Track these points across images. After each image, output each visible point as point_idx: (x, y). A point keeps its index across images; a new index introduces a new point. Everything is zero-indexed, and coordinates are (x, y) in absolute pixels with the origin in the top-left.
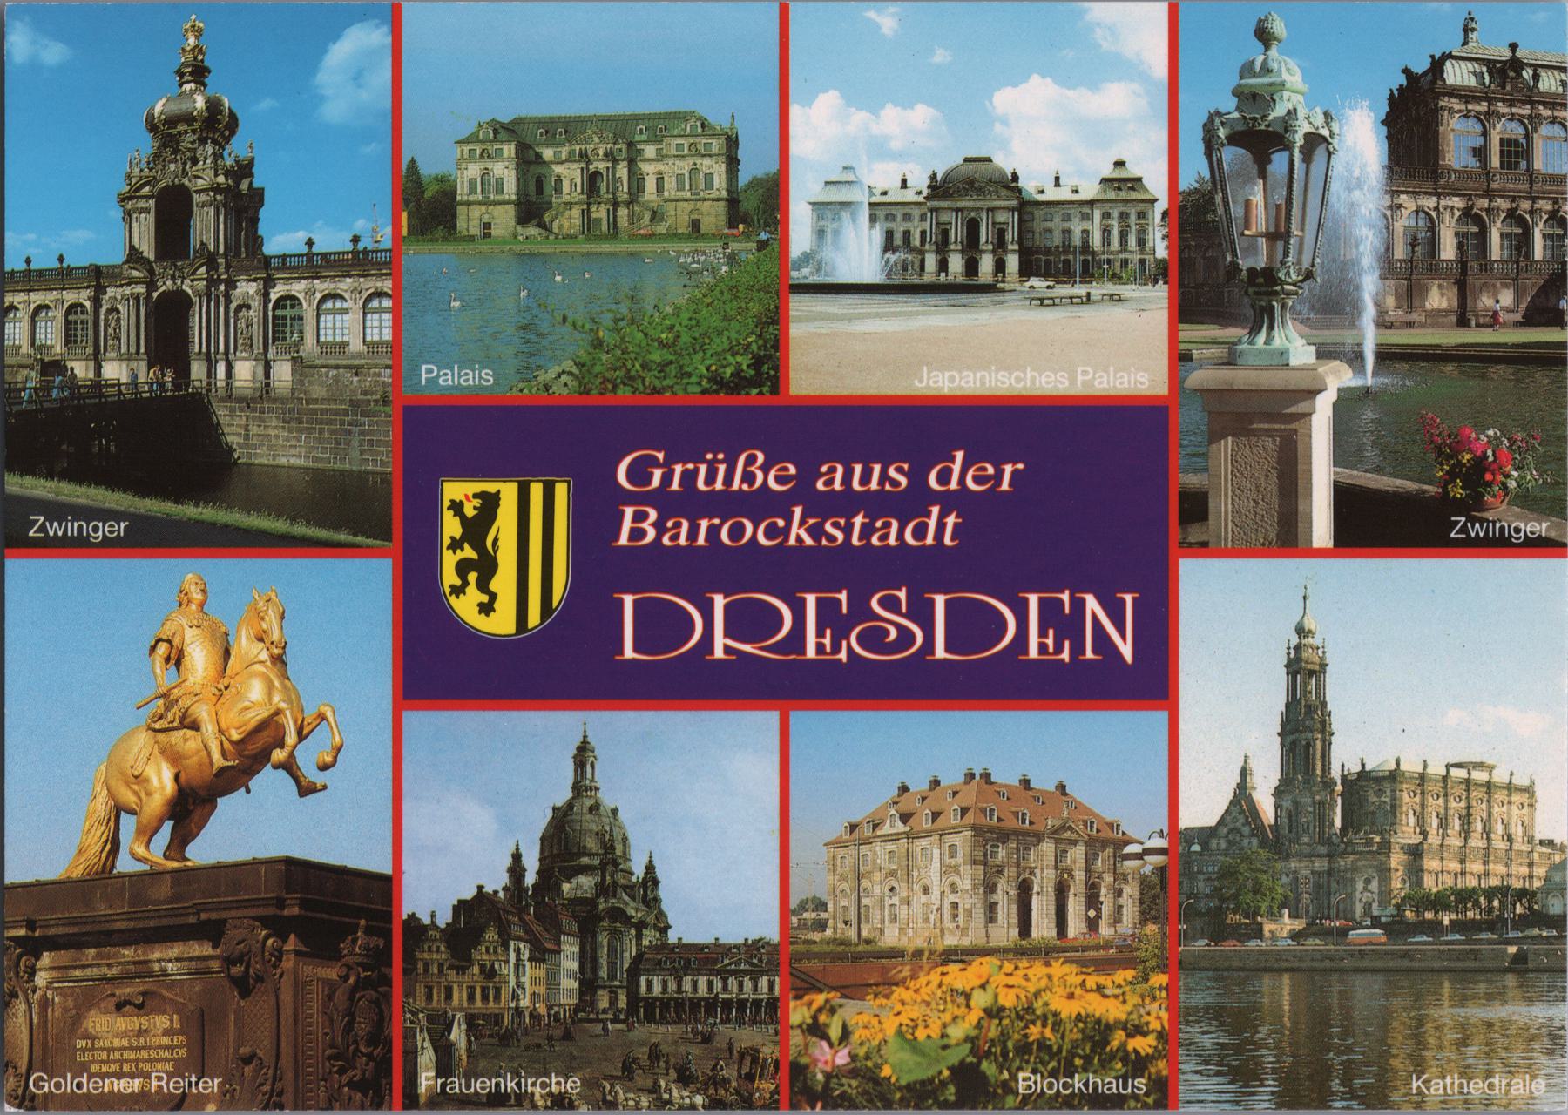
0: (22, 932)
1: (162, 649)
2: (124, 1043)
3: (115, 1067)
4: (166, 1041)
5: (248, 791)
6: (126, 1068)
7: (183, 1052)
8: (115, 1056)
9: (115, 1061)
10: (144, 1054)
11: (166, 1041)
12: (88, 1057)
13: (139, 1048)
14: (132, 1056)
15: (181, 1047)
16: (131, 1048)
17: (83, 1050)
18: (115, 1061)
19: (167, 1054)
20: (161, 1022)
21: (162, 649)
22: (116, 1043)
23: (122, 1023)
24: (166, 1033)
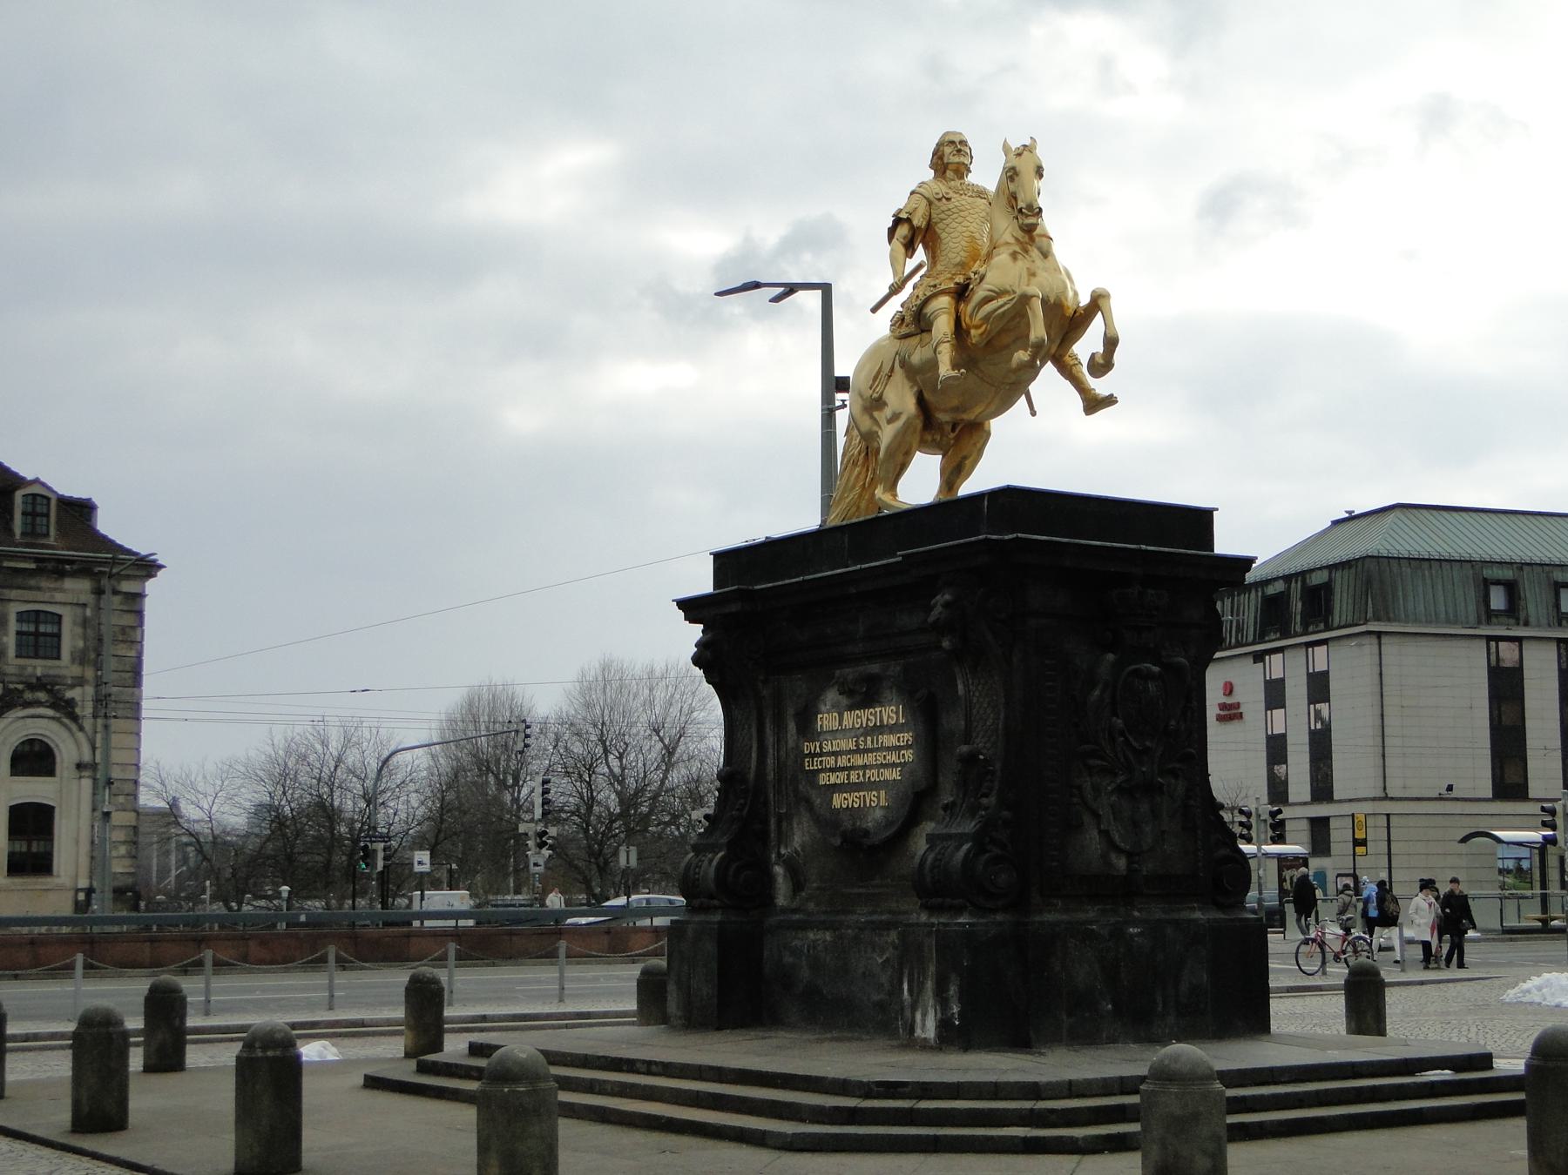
0: (734, 608)
1: (903, 230)
4: (889, 740)
5: (1033, 413)
6: (854, 778)
8: (842, 761)
10: (869, 759)
14: (860, 762)
15: (907, 747)
16: (858, 751)
17: (812, 755)
19: (893, 758)
20: (890, 713)
21: (903, 230)
23: (850, 719)
24: (893, 729)
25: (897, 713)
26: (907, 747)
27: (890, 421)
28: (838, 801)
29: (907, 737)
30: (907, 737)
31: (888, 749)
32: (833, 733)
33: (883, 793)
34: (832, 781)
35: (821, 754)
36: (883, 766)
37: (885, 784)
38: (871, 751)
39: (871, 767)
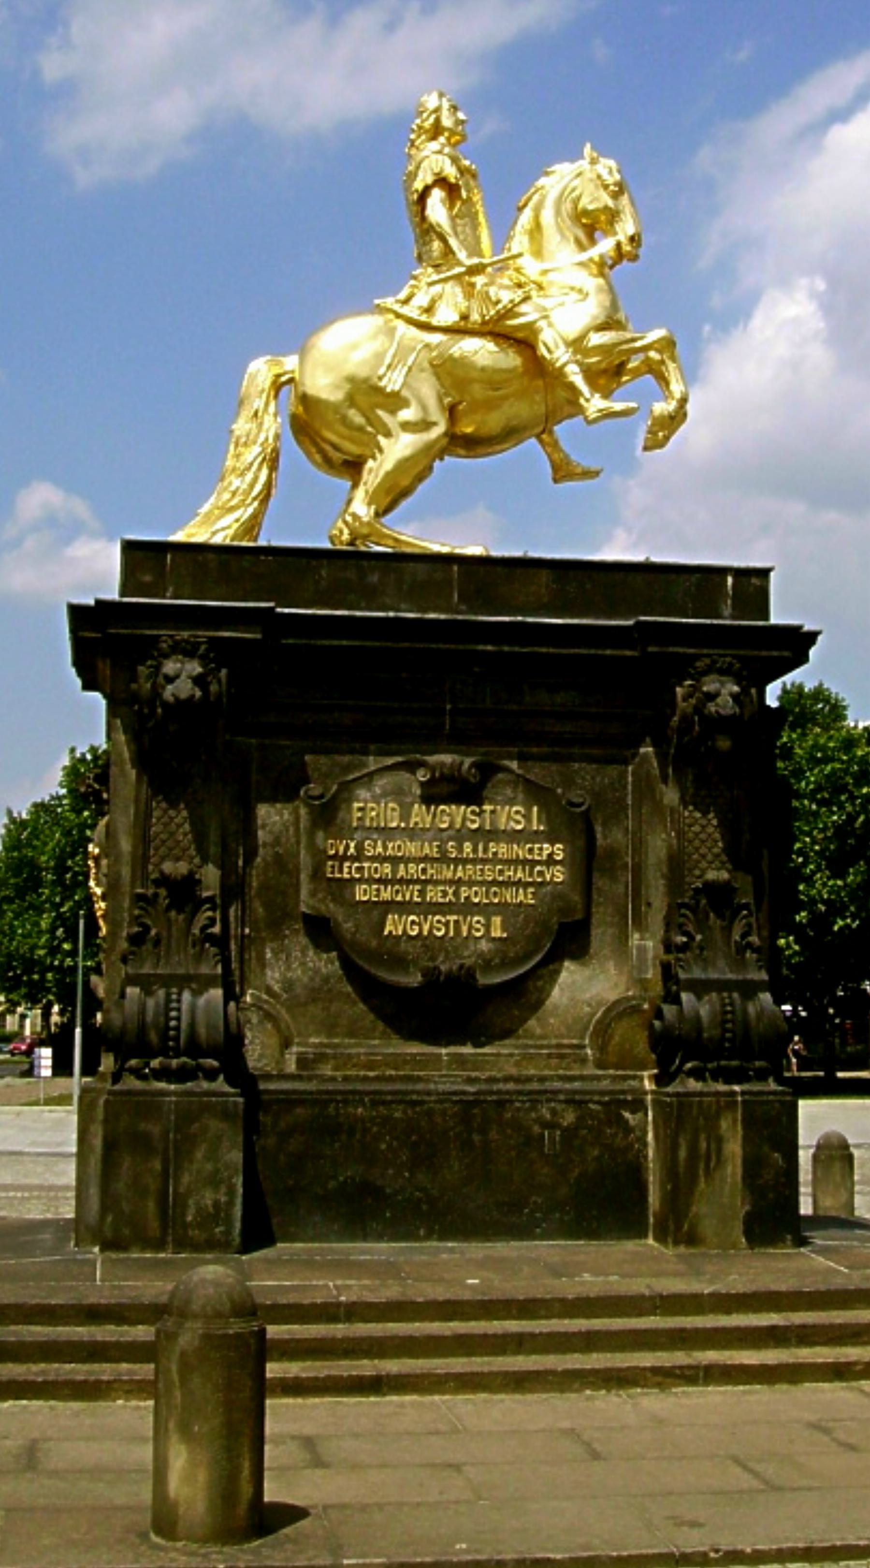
2: (430, 849)
3: (412, 894)
4: (519, 851)
6: (434, 894)
7: (558, 875)
9: (409, 882)
11: (519, 851)
12: (348, 871)
13: (465, 861)
15: (550, 861)
16: (443, 859)
18: (409, 882)
20: (512, 815)
22: (412, 848)
23: (420, 815)
24: (514, 837)
25: (527, 817)
26: (550, 861)
27: (406, 426)
28: (393, 925)
29: (559, 851)
30: (559, 851)
31: (508, 862)
32: (386, 833)
33: (497, 920)
34: (386, 894)
35: (359, 857)
36: (494, 883)
37: (502, 908)
38: (474, 861)
39: (471, 883)
